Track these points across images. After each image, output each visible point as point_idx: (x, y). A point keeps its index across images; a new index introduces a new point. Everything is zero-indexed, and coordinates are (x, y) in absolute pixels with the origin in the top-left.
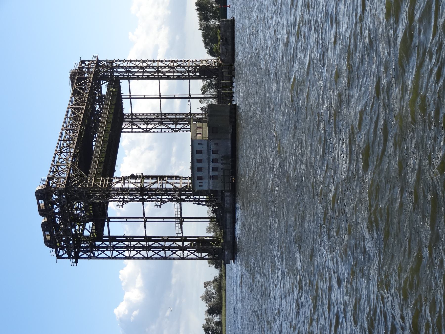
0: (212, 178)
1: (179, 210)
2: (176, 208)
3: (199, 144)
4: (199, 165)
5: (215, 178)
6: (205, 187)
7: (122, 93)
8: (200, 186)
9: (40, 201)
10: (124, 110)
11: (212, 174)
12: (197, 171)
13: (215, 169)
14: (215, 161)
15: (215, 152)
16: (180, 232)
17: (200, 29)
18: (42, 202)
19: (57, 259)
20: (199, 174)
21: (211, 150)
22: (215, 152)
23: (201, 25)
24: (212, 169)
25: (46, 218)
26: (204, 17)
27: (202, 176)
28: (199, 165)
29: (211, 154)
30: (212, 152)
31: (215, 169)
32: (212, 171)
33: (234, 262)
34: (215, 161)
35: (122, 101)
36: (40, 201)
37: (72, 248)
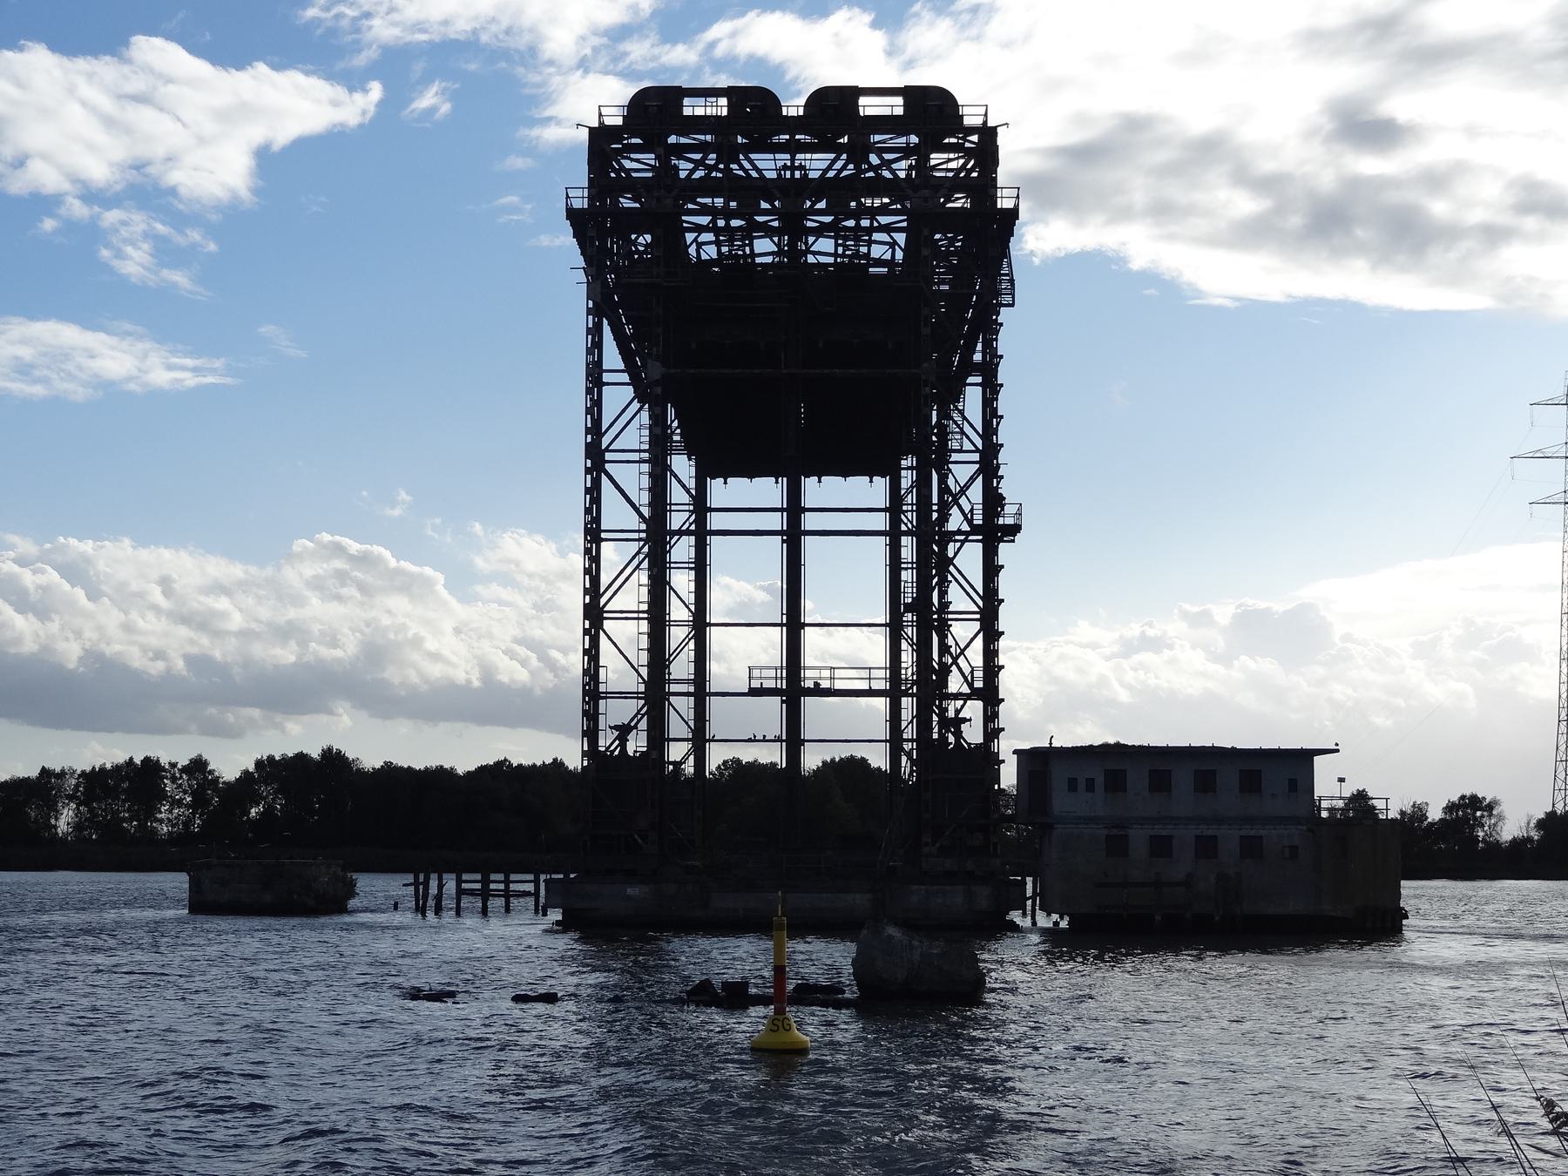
0: (1115, 831)
1: (863, 685)
2: (838, 673)
3: (1293, 785)
4: (1183, 779)
5: (1117, 845)
6: (1062, 802)
7: (823, 478)
8: (1072, 785)
9: (899, 100)
10: (746, 480)
11: (1138, 838)
12: (1150, 771)
13: (1161, 847)
14: (1206, 847)
15: (1251, 847)
16: (756, 684)
17: (44, 771)
19: (592, 131)
20: (1138, 779)
21: (1263, 832)
22: (1251, 847)
23: (62, 774)
24: (1164, 833)
25: (801, 113)
26: (98, 782)
27: (1125, 790)
28: (1138, 779)
29: (1243, 833)
30: (1252, 833)
31: (1161, 847)
32: (1153, 833)
33: (558, 923)
34: (1206, 847)
35: (883, 476)
36: (899, 100)
37: (658, 199)
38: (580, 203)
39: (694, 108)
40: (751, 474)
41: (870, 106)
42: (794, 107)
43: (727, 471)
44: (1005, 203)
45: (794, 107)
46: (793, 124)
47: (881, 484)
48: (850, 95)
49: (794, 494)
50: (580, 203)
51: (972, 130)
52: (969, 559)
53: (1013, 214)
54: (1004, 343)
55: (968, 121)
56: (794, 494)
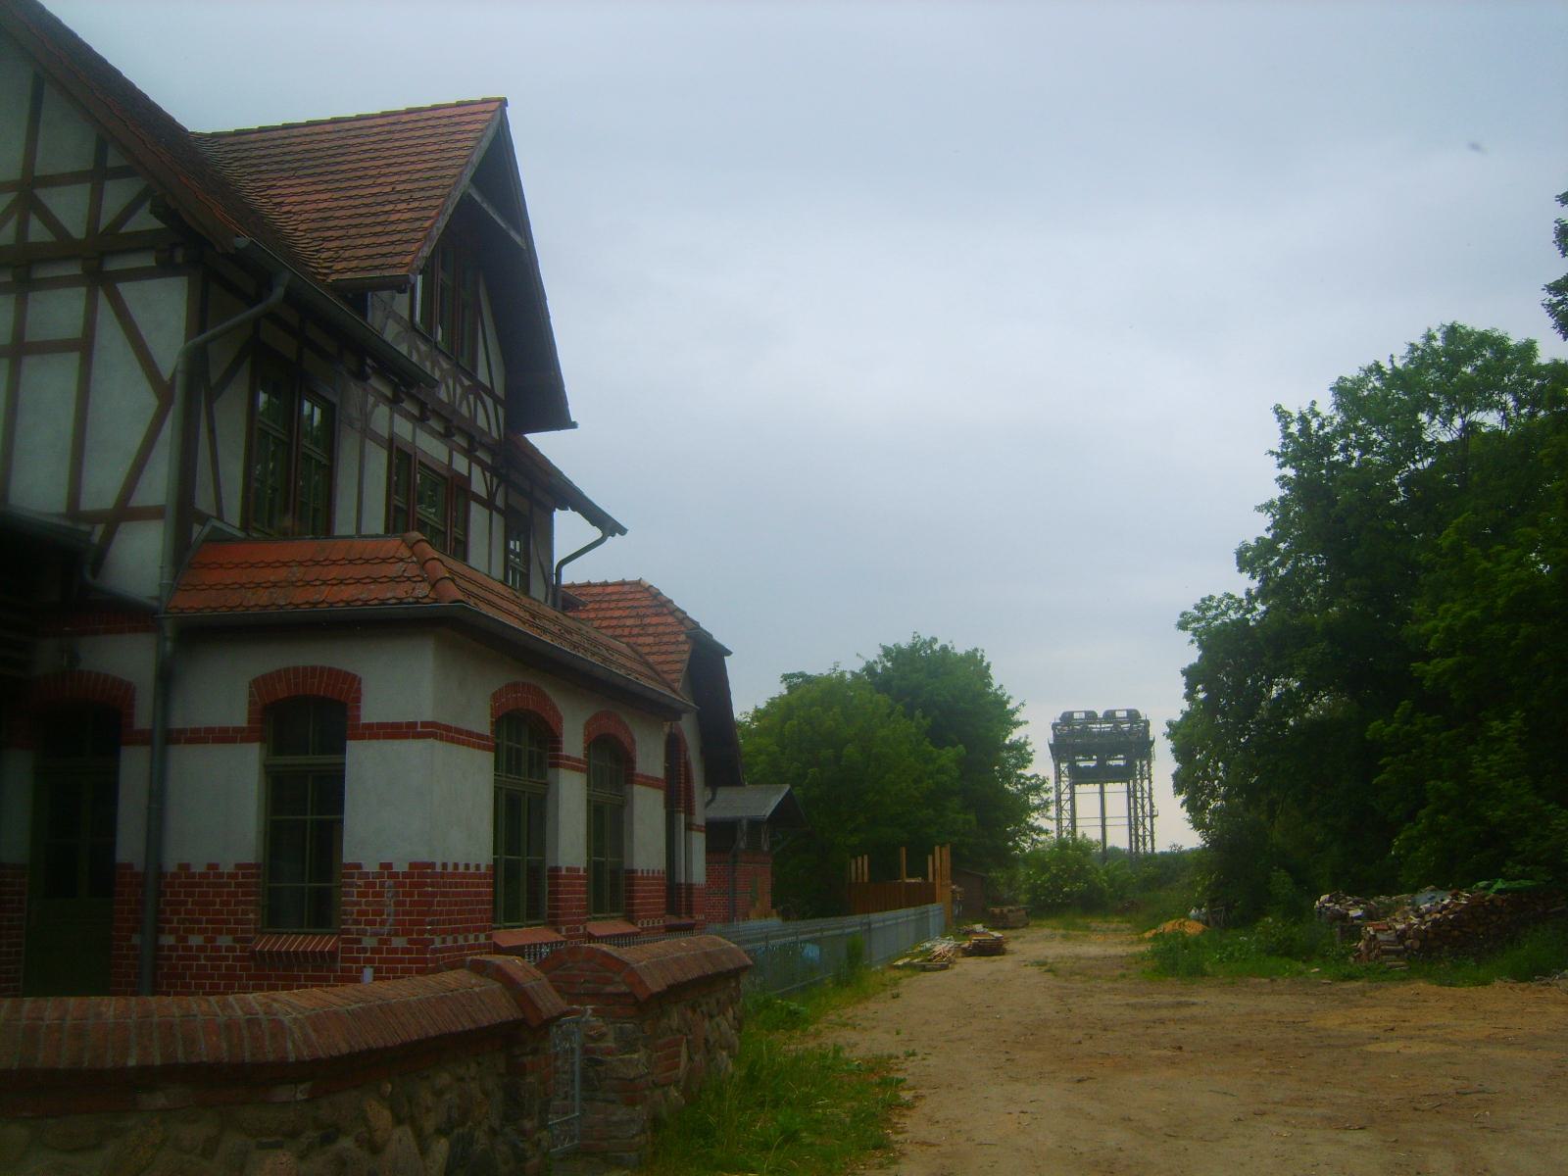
18: (1125, 714)
38: (1052, 742)
39: (1076, 716)
40: (1087, 783)
41: (1118, 714)
42: (1100, 715)
43: (1080, 783)
44: (1151, 739)
45: (1100, 715)
46: (1100, 719)
47: (1125, 785)
48: (1113, 712)
49: (1102, 788)
50: (1052, 742)
51: (1142, 721)
52: (1147, 821)
53: (1153, 741)
54: (1153, 771)
55: (1143, 718)
56: (1102, 788)
